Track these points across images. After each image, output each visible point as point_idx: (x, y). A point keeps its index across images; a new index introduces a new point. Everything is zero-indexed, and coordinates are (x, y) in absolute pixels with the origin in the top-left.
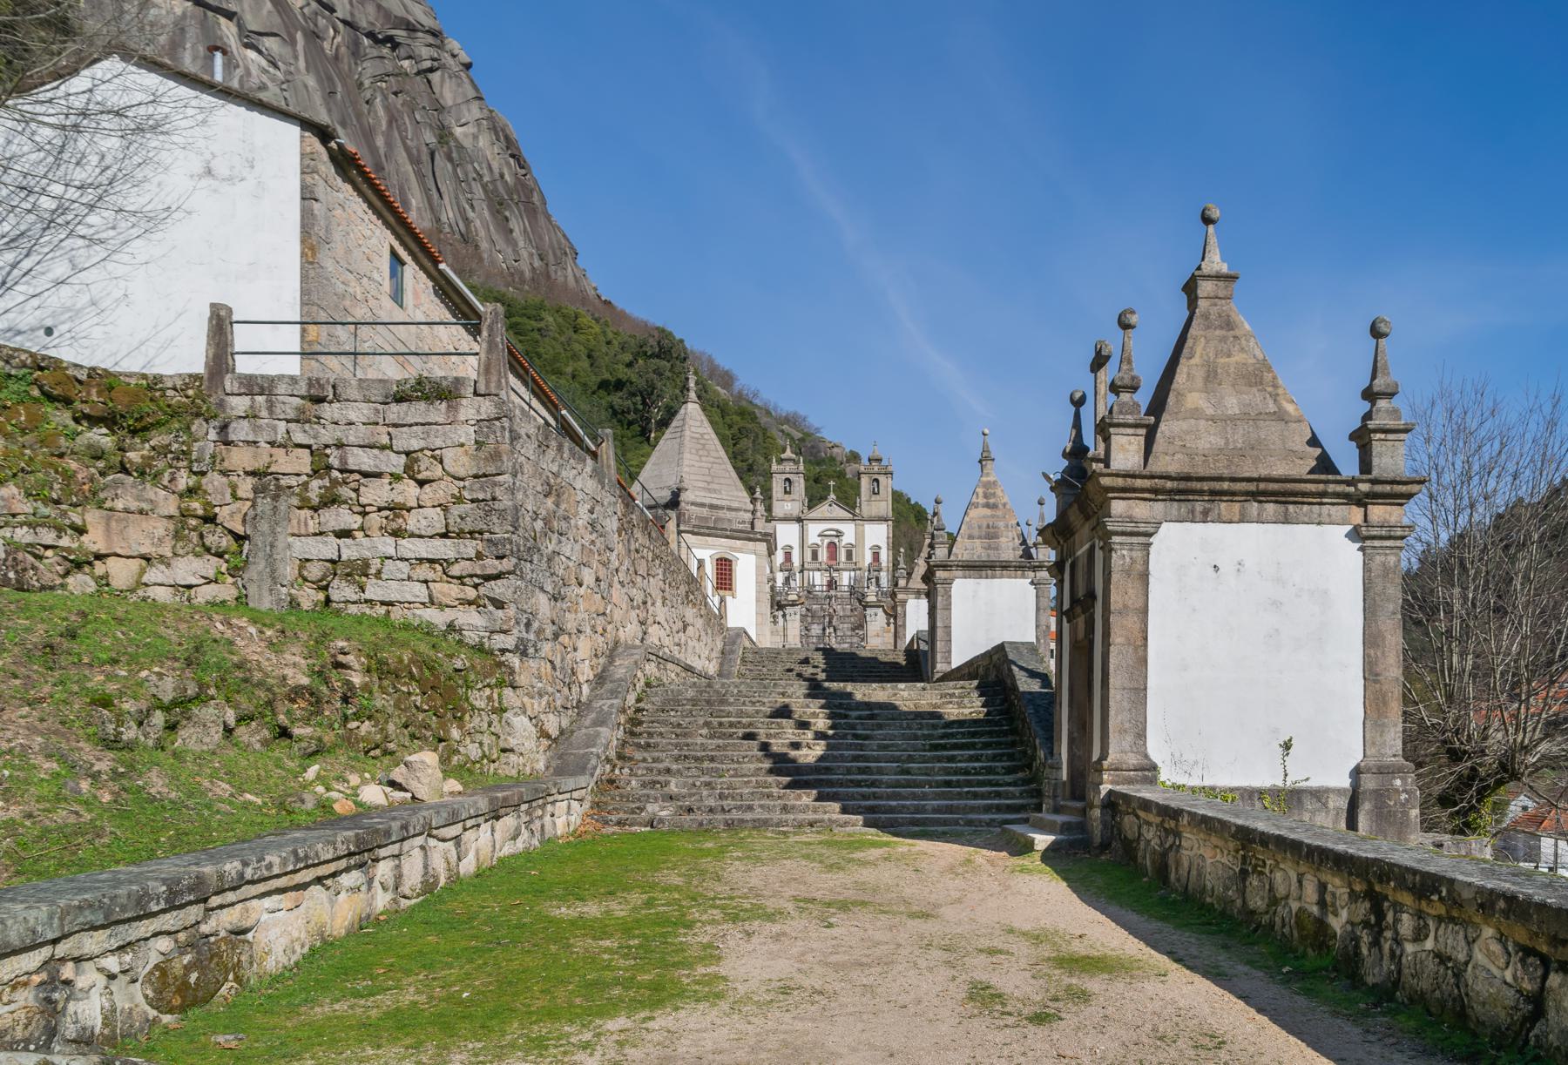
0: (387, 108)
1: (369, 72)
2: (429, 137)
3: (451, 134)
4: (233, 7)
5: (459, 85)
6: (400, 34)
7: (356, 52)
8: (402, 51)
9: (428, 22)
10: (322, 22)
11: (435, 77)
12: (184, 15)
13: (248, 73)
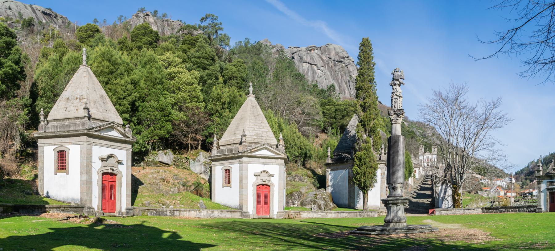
0: (341, 74)
1: (337, 69)
2: (348, 78)
3: (352, 77)
4: (316, 64)
5: (353, 67)
6: (342, 60)
7: (335, 65)
8: (343, 63)
9: (347, 56)
10: (329, 61)
11: (349, 66)
12: (308, 67)
13: (319, 74)
